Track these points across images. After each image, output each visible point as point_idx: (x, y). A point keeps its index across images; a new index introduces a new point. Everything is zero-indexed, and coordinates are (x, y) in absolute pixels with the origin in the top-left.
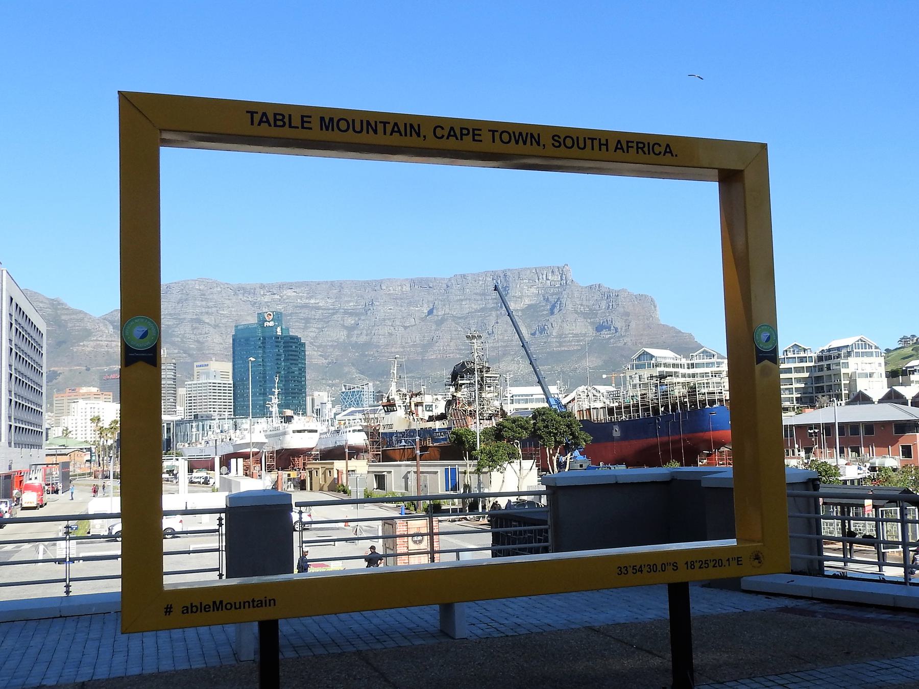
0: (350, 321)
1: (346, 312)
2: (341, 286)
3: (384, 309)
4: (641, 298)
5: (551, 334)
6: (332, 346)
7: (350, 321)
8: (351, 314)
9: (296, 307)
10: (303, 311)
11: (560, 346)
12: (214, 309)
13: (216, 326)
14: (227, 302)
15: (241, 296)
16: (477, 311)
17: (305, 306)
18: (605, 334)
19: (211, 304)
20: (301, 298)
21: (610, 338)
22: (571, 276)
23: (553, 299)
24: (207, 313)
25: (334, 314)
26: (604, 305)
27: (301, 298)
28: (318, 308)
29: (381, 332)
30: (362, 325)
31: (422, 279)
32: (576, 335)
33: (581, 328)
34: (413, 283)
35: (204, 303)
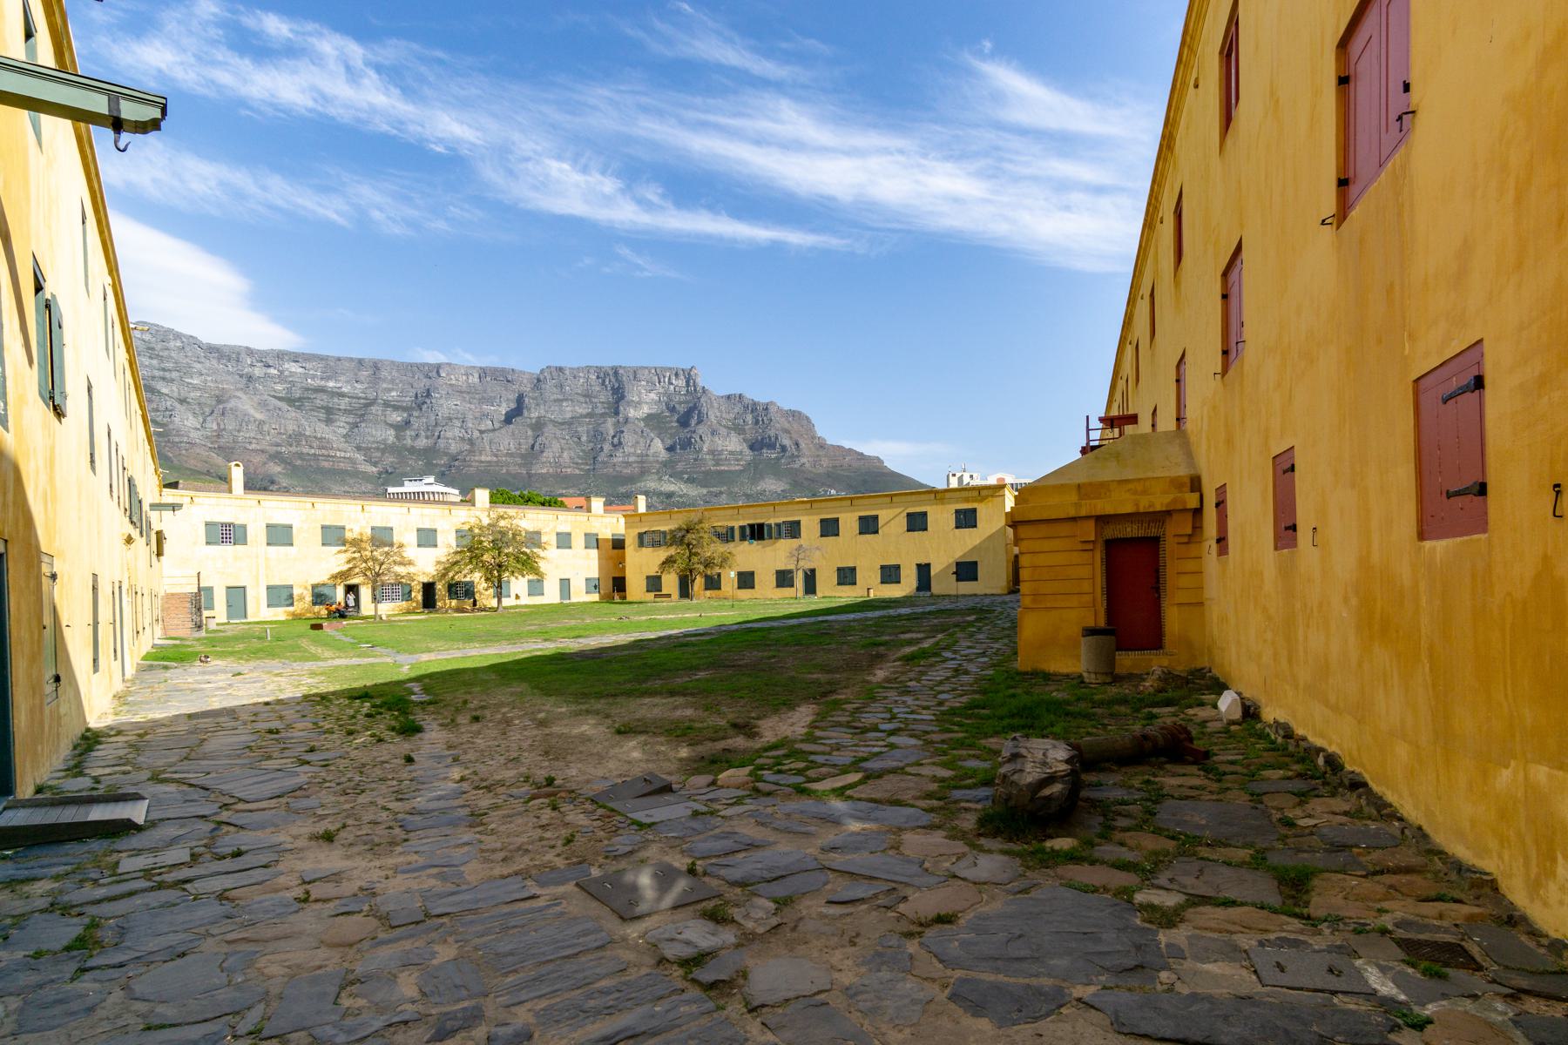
0: (397, 417)
1: (387, 404)
2: (376, 366)
3: (446, 405)
4: (795, 415)
5: (701, 449)
6: (377, 449)
7: (397, 417)
8: (396, 408)
9: (307, 389)
10: (319, 395)
11: (717, 464)
12: (175, 375)
13: (182, 401)
14: (198, 366)
15: (214, 362)
16: (582, 416)
17: (321, 390)
18: (767, 454)
19: (170, 365)
20: (313, 377)
21: (778, 459)
22: (701, 382)
23: (682, 409)
24: (164, 379)
25: (367, 406)
26: (749, 418)
27: (313, 377)
28: (342, 395)
29: (449, 434)
30: (415, 424)
31: (496, 370)
32: (731, 453)
33: (733, 444)
34: (484, 373)
35: (155, 362)
